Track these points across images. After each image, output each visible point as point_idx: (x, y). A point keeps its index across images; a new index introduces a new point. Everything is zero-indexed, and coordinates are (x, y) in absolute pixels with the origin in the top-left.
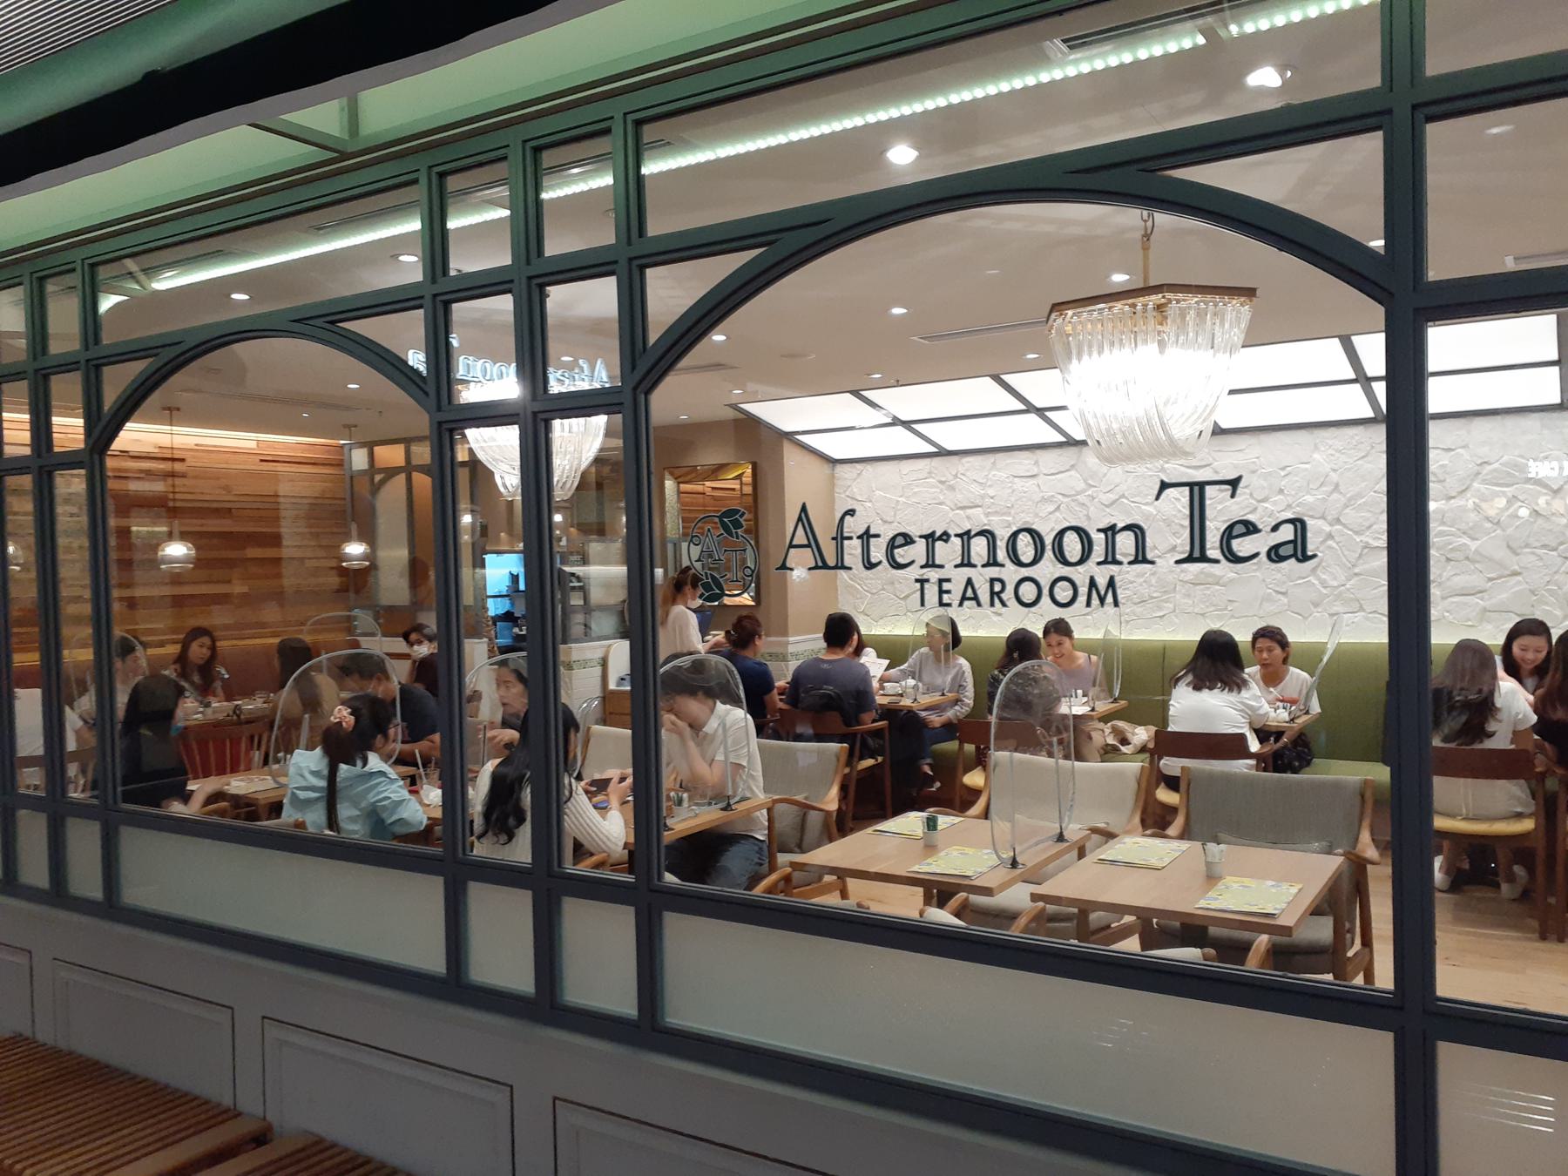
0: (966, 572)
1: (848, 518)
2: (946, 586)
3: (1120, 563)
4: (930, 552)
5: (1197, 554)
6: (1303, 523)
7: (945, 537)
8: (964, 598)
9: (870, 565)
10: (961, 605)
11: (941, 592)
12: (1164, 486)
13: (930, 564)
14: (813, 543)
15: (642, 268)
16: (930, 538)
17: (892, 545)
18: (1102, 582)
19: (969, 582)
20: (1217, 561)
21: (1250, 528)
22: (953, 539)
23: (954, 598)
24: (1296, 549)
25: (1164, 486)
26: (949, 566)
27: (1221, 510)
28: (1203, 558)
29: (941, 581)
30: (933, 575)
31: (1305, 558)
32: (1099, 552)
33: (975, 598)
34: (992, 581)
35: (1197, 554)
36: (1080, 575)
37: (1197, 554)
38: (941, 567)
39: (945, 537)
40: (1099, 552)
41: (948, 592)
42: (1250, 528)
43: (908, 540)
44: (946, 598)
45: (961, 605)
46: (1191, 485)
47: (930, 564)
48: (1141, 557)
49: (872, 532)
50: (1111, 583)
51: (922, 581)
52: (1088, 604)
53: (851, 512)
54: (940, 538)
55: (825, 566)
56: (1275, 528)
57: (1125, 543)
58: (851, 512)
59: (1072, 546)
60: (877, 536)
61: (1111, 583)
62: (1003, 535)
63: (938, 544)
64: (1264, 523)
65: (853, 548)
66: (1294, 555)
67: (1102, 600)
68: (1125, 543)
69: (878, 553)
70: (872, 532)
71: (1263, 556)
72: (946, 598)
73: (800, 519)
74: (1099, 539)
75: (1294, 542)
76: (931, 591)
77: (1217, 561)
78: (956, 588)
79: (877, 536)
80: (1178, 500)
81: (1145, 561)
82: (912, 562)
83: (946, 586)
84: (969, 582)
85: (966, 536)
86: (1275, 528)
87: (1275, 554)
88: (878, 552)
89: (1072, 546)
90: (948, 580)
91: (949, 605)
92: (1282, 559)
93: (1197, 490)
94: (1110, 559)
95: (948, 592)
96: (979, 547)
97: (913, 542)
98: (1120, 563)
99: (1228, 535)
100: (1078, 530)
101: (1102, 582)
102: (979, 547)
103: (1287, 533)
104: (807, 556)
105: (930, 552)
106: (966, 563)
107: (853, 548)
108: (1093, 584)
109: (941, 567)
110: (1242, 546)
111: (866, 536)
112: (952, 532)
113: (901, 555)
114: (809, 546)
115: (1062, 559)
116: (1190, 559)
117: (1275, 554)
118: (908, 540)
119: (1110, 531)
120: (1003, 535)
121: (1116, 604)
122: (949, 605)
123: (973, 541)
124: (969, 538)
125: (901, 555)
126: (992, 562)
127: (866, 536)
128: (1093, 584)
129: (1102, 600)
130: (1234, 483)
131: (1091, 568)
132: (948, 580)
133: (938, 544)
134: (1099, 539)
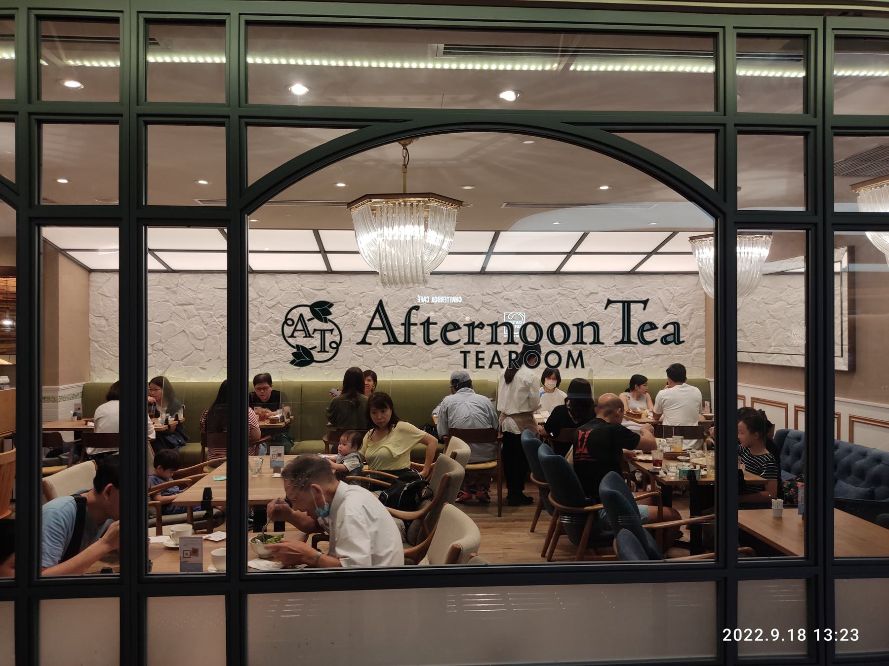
0: (495, 347)
1: (414, 311)
2: (481, 356)
3: (585, 344)
4: (471, 335)
5: (626, 339)
6: (678, 324)
7: (481, 326)
8: (492, 363)
9: (428, 342)
10: (490, 367)
11: (478, 359)
12: (609, 302)
13: (471, 341)
14: (387, 326)
15: (716, 132)
16: (471, 326)
17: (445, 330)
18: (575, 355)
19: (496, 353)
20: (636, 343)
21: (653, 326)
22: (486, 327)
23: (488, 362)
24: (674, 337)
25: (609, 302)
26: (483, 344)
27: (638, 316)
28: (629, 342)
29: (478, 353)
30: (472, 348)
31: (679, 342)
32: (573, 337)
33: (500, 363)
34: (511, 353)
35: (626, 340)
36: (563, 350)
37: (626, 340)
38: (479, 344)
39: (481, 326)
40: (573, 337)
41: (483, 359)
42: (653, 326)
43: (456, 327)
44: (481, 363)
45: (490, 367)
46: (623, 302)
47: (471, 341)
48: (597, 341)
49: (431, 321)
50: (580, 355)
51: (465, 353)
52: (567, 367)
53: (417, 308)
54: (478, 326)
55: (396, 342)
56: (665, 327)
57: (588, 331)
58: (417, 308)
59: (558, 332)
60: (436, 324)
61: (580, 355)
62: (517, 326)
63: (477, 330)
64: (660, 325)
65: (417, 334)
66: (674, 341)
67: (575, 364)
68: (588, 331)
69: (435, 332)
70: (431, 321)
71: (659, 341)
72: (481, 363)
73: (377, 311)
74: (574, 331)
75: (674, 334)
76: (471, 358)
77: (636, 343)
78: (488, 356)
79: (436, 324)
80: (616, 311)
81: (599, 343)
82: (459, 341)
83: (481, 356)
84: (496, 353)
85: (495, 326)
86: (665, 327)
87: (665, 341)
88: (435, 332)
89: (558, 332)
90: (483, 352)
91: (483, 367)
92: (668, 343)
93: (627, 305)
94: (580, 341)
95: (483, 359)
96: (503, 333)
97: (459, 328)
98: (585, 344)
99: (642, 330)
100: (563, 325)
101: (575, 355)
102: (503, 333)
103: (671, 328)
104: (383, 336)
105: (471, 335)
106: (494, 341)
107: (417, 334)
108: (570, 354)
109: (479, 344)
110: (648, 336)
111: (427, 324)
112: (485, 323)
113: (648, 336)
114: (384, 328)
115: (553, 341)
116: (622, 342)
117: (665, 341)
118: (456, 327)
119: (580, 326)
120: (517, 326)
121: (583, 366)
122: (483, 367)
123: (499, 329)
124: (497, 327)
125: (452, 336)
126: (511, 341)
127: (427, 324)
128: (570, 354)
129: (575, 364)
130: (645, 302)
131: (568, 347)
132: (483, 352)
133: (477, 330)
134: (574, 331)
